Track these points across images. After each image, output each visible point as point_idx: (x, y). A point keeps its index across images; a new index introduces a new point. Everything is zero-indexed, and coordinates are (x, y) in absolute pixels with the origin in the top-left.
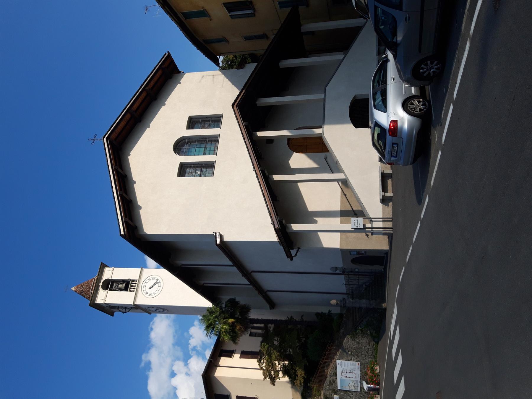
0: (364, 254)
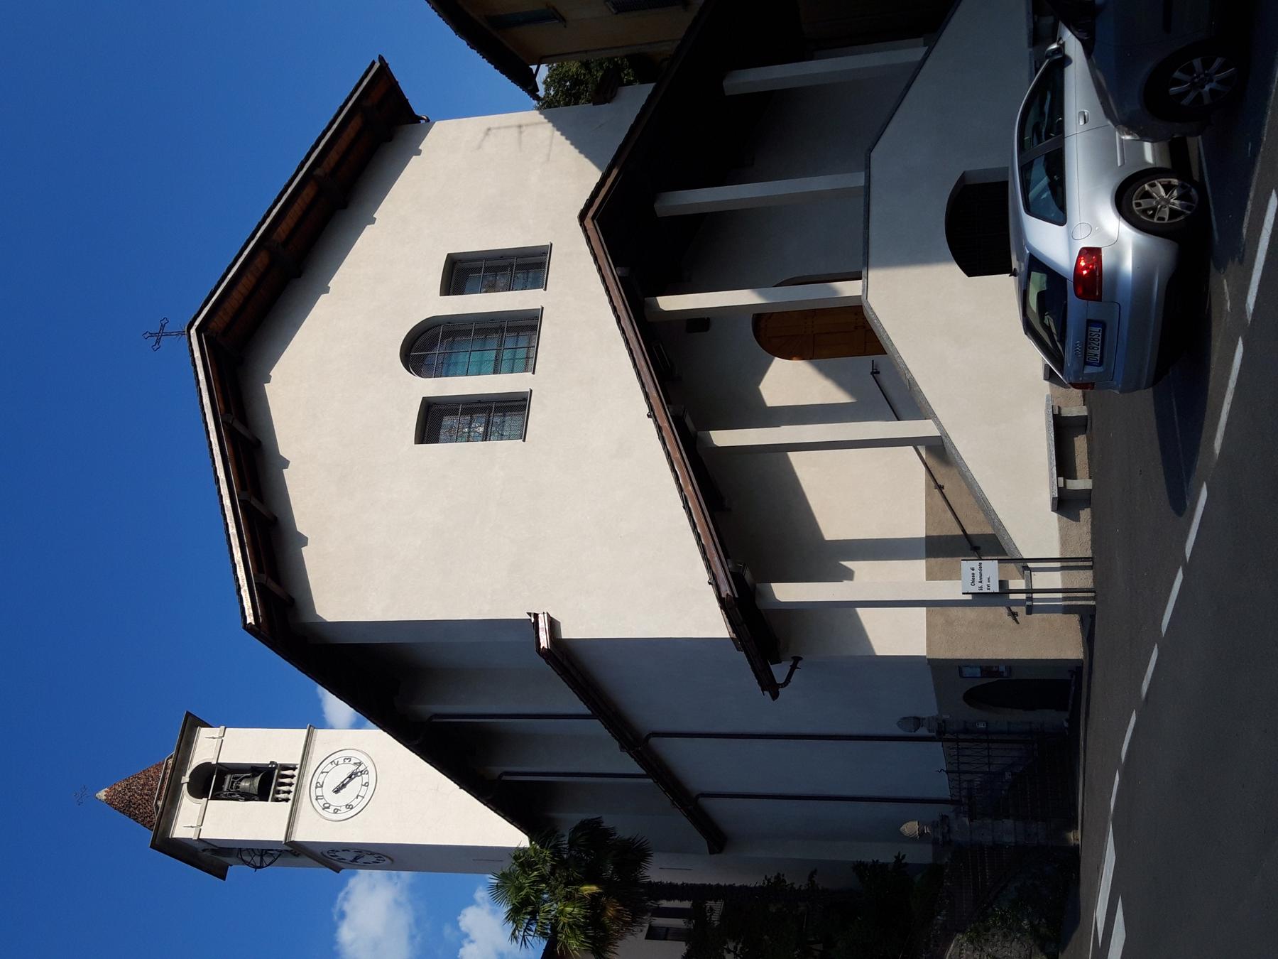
0: (1005, 674)
